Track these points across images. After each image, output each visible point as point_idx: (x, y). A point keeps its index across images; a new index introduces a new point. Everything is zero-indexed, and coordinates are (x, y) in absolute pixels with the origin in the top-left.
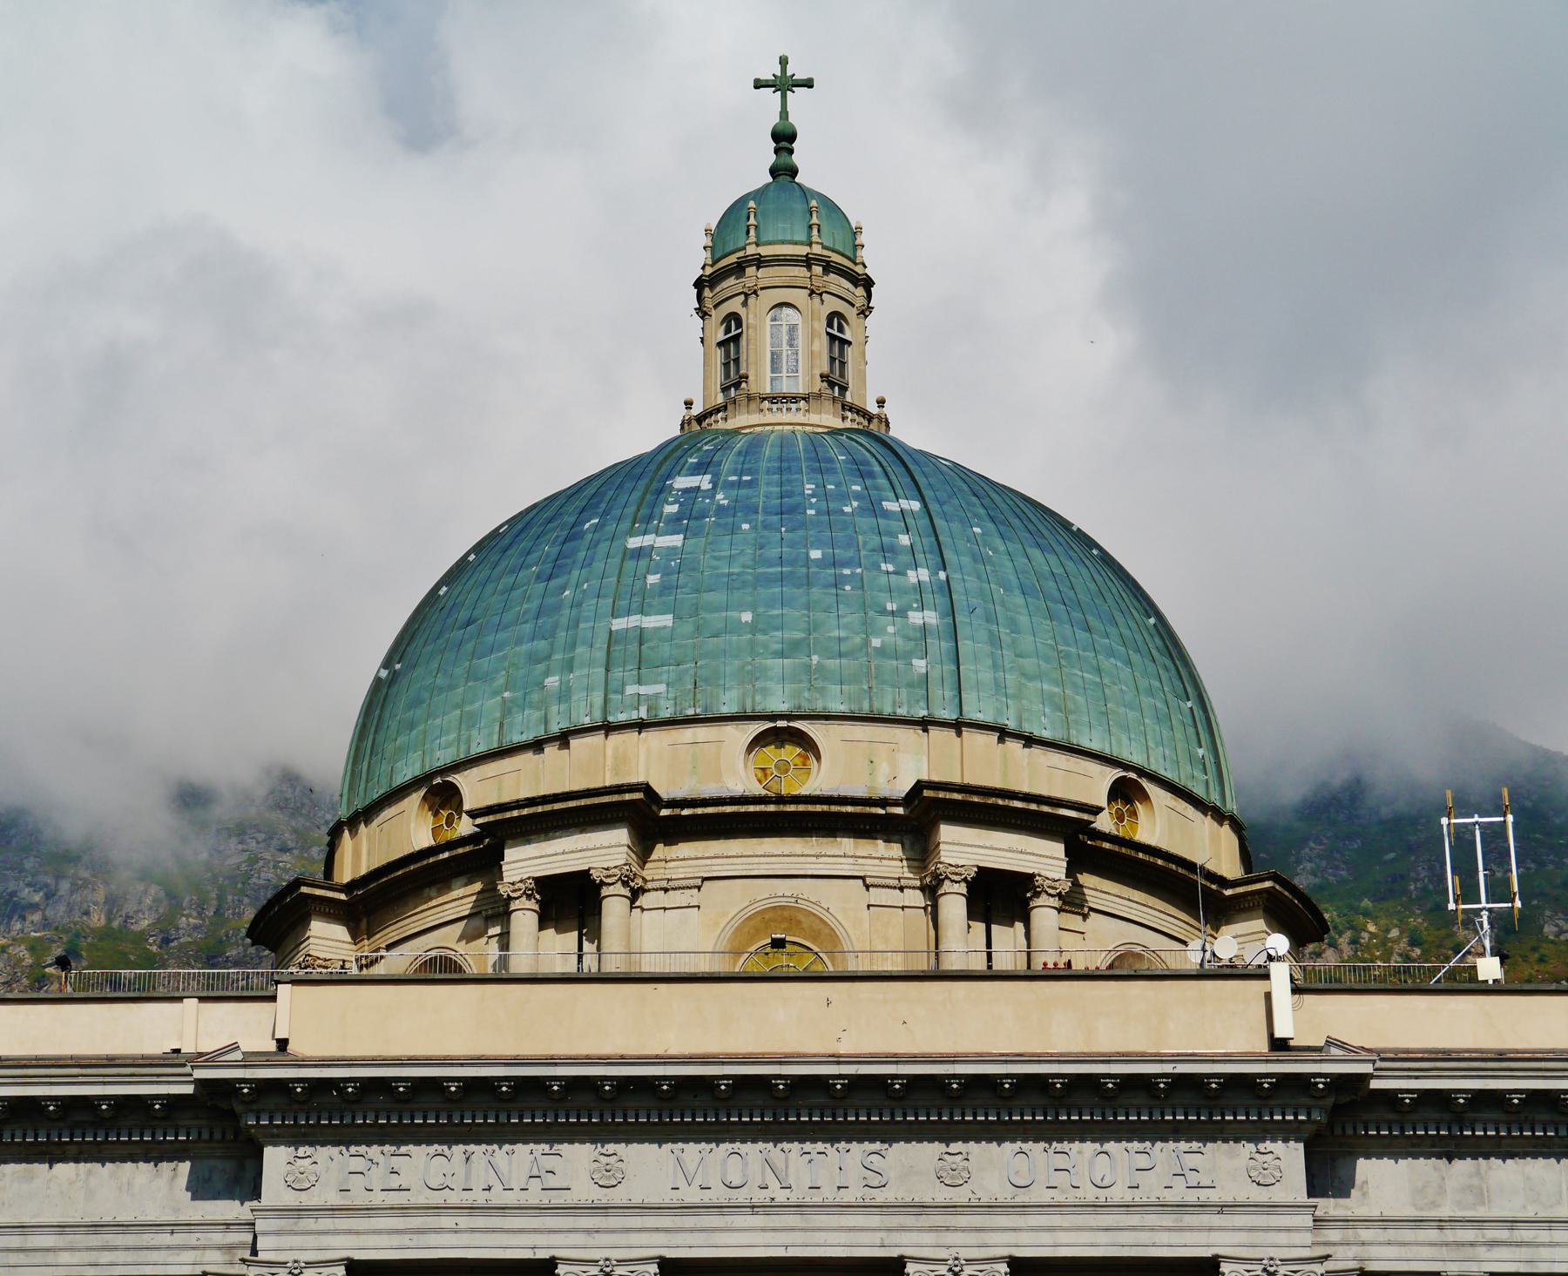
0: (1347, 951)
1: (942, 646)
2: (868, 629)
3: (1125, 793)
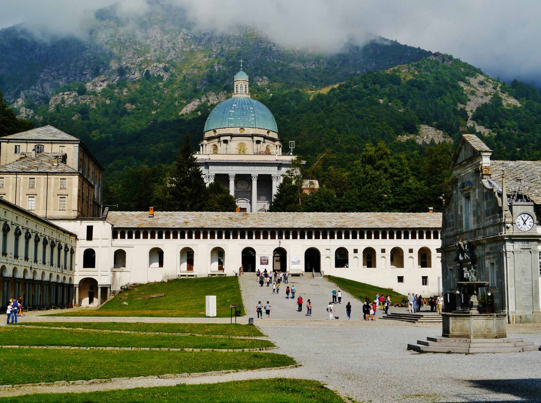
0: (317, 65)
1: (254, 121)
2: (249, 120)
3: (268, 132)
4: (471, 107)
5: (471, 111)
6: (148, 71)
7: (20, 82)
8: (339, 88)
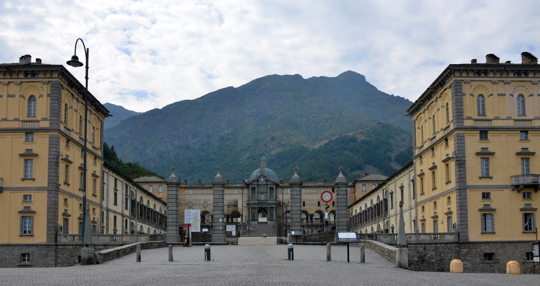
4: (393, 156)
5: (395, 156)
6: (222, 136)
7: (154, 143)
8: (325, 144)
